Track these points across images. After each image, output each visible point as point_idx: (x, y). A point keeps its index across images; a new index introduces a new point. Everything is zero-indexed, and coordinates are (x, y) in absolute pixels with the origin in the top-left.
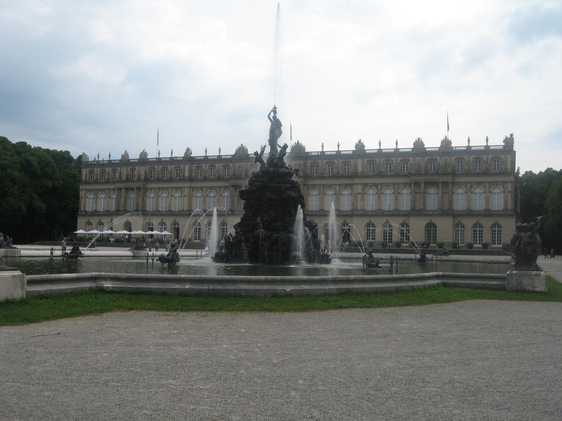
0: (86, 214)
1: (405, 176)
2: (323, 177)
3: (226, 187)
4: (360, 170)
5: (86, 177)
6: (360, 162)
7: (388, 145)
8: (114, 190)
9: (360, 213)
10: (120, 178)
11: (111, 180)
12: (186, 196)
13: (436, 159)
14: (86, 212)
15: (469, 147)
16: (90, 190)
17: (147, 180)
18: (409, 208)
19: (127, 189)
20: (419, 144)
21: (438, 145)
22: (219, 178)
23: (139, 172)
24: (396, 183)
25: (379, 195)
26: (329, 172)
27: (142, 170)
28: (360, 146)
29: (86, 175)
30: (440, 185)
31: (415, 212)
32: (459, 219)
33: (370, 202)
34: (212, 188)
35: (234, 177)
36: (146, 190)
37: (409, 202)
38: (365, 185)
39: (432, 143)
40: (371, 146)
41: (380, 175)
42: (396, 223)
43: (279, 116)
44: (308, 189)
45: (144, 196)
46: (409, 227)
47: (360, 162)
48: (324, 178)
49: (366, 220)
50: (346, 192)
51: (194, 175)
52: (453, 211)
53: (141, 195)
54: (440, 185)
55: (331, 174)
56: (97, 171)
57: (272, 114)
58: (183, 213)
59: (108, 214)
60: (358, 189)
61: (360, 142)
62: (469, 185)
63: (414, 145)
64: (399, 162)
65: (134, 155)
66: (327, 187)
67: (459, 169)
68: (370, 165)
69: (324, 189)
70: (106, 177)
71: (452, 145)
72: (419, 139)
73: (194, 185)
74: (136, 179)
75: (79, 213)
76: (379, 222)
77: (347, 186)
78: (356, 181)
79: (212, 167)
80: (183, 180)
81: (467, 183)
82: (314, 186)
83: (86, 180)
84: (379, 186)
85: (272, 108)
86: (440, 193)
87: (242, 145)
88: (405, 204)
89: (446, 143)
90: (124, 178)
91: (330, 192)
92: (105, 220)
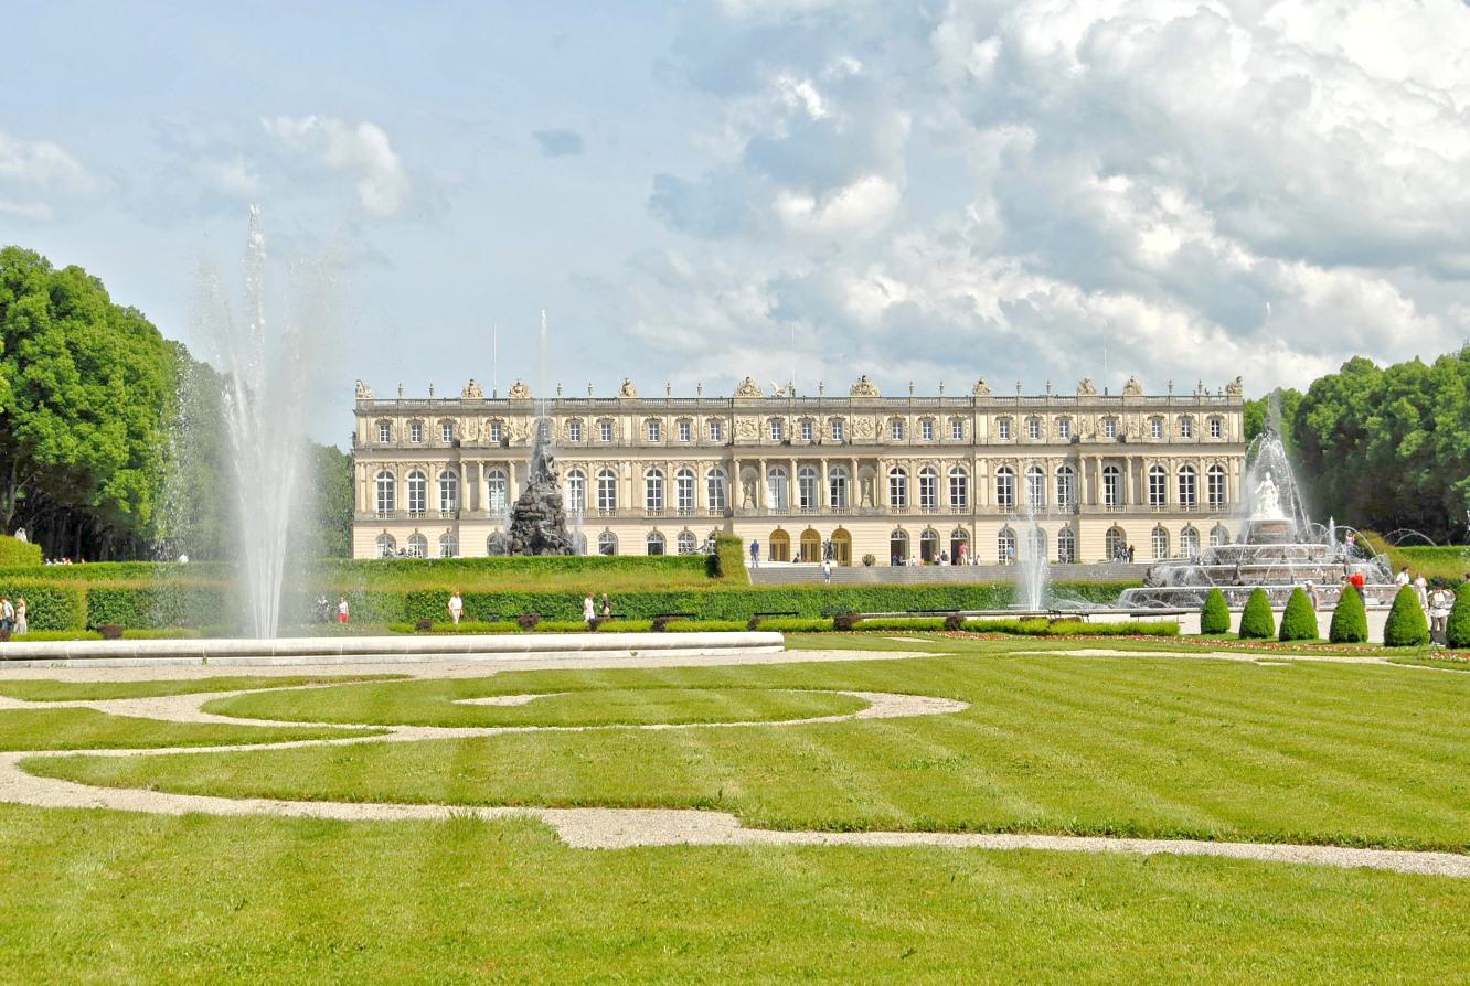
4: (983, 432)
5: (368, 436)
9: (987, 513)
12: (628, 479)
35: (741, 443)
47: (982, 419)
55: (927, 441)
58: (626, 515)
63: (1079, 390)
75: (357, 516)
80: (620, 448)
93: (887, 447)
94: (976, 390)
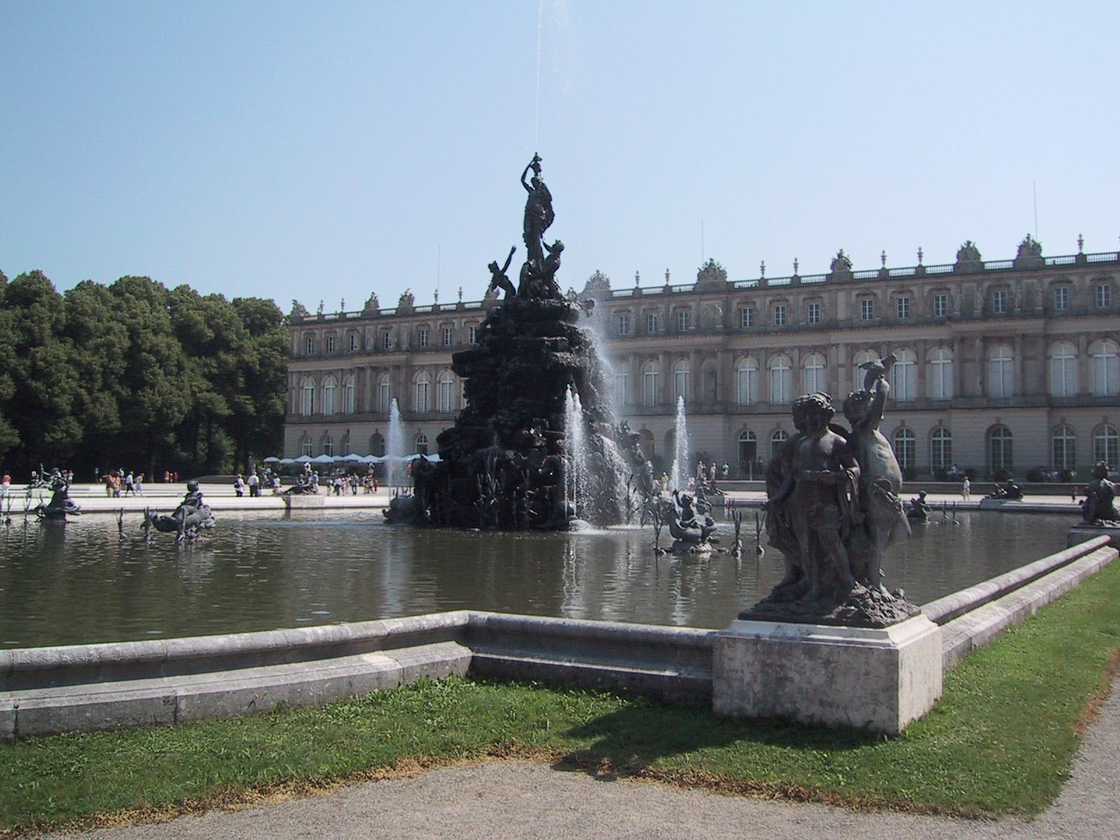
0: (301, 420)
1: (940, 323)
4: (842, 315)
5: (299, 349)
6: (841, 297)
7: (902, 261)
8: (351, 371)
10: (363, 347)
11: (345, 352)
13: (1008, 286)
18: (950, 394)
20: (968, 254)
21: (1013, 254)
23: (398, 336)
24: (921, 341)
26: (778, 322)
27: (405, 329)
28: (841, 263)
29: (299, 344)
30: (1018, 340)
31: (964, 400)
32: (1063, 413)
36: (411, 370)
37: (950, 380)
39: (998, 251)
40: (864, 264)
41: (887, 324)
43: (546, 177)
44: (735, 358)
46: (950, 435)
47: (841, 297)
48: (766, 333)
52: (1048, 396)
53: (402, 378)
54: (1018, 340)
56: (320, 334)
57: (531, 173)
59: (341, 419)
61: (840, 256)
62: (1083, 340)
63: (958, 257)
64: (926, 294)
66: (773, 353)
67: (1059, 305)
68: (864, 303)
69: (767, 358)
70: (337, 348)
71: (1043, 254)
72: (969, 243)
74: (391, 347)
77: (814, 349)
78: (835, 337)
81: (1079, 334)
82: (746, 352)
83: (299, 353)
84: (884, 348)
85: (529, 160)
86: (1018, 358)
87: (598, 271)
88: (942, 384)
89: (1029, 249)
90: (369, 348)
92: (336, 432)
94: (833, 267)
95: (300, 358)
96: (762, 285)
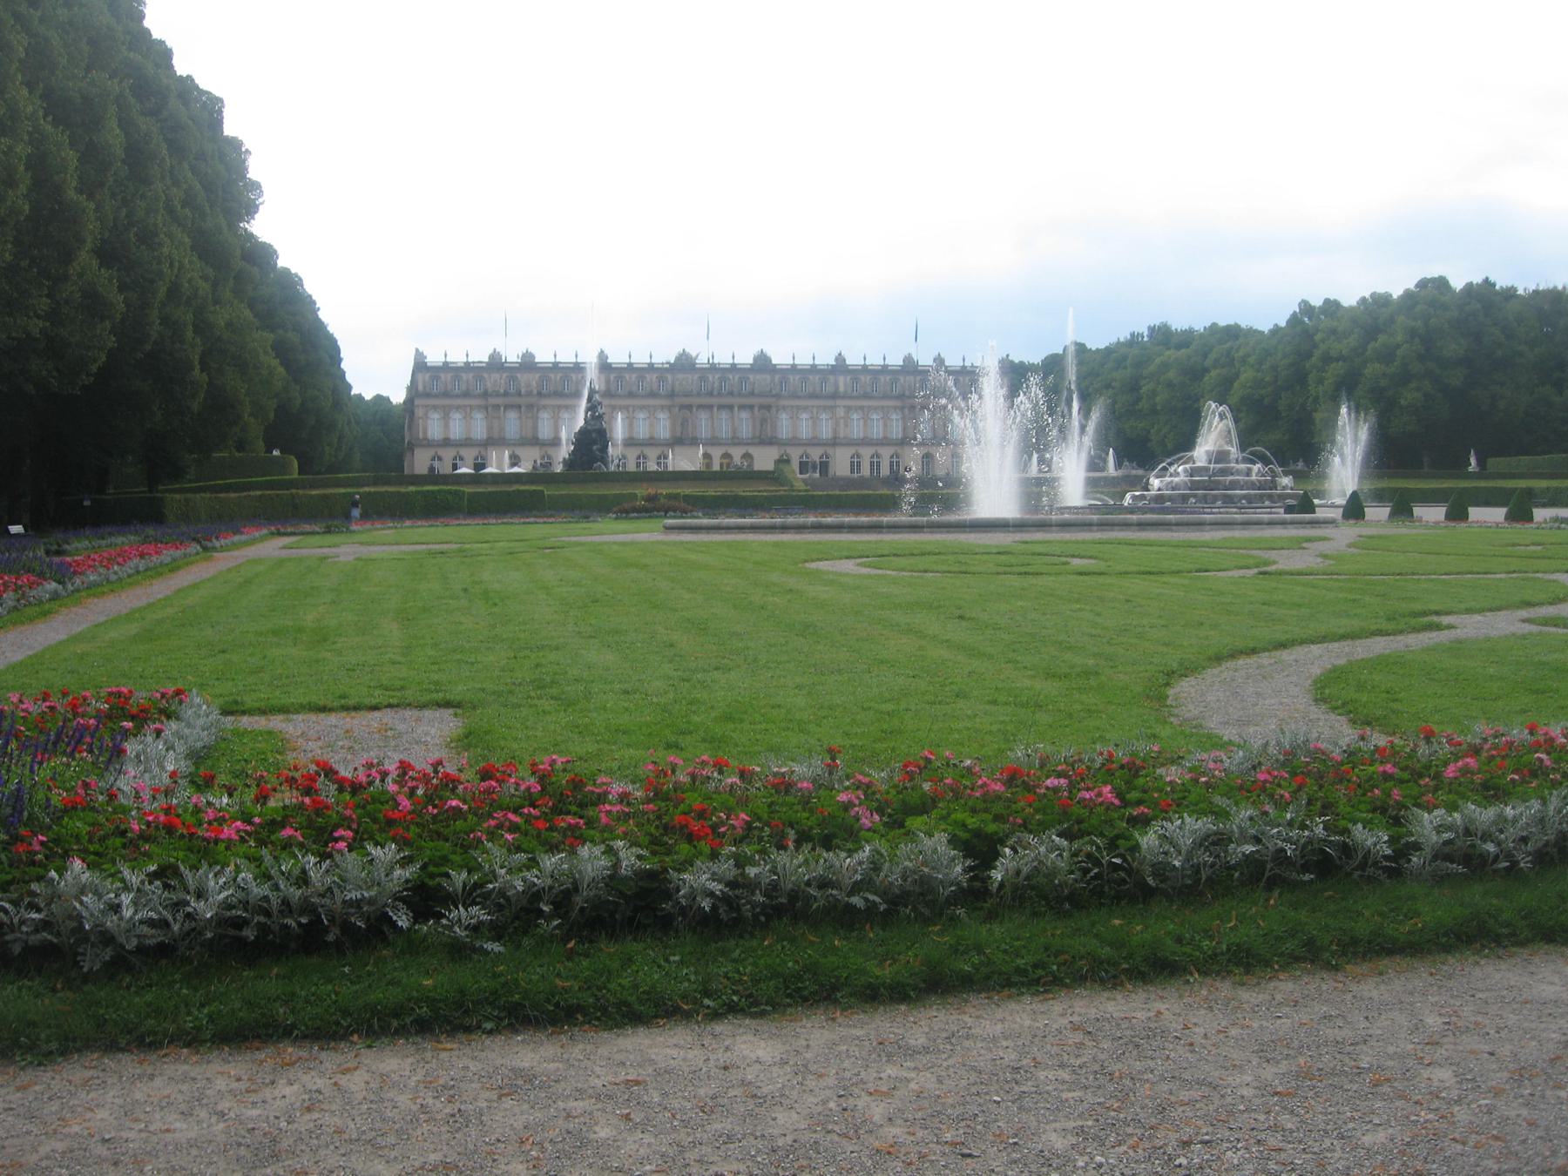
0: (428, 444)
2: (795, 396)
3: (662, 407)
4: (842, 389)
6: (841, 379)
14: (426, 439)
15: (964, 367)
16: (435, 408)
17: (540, 394)
19: (507, 407)
22: (653, 395)
25: (866, 420)
27: (528, 380)
28: (840, 358)
33: (856, 430)
34: (642, 408)
38: (848, 409)
40: (853, 360)
41: (866, 396)
42: (886, 453)
45: (536, 419)
47: (841, 379)
48: (799, 397)
49: (852, 450)
50: (824, 416)
51: (613, 388)
60: (841, 412)
65: (512, 356)
73: (614, 402)
76: (866, 453)
77: (825, 408)
78: (839, 402)
79: (641, 378)
82: (784, 408)
88: (896, 432)
91: (804, 416)
93: (778, 396)
95: (428, 395)
96: (794, 368)
